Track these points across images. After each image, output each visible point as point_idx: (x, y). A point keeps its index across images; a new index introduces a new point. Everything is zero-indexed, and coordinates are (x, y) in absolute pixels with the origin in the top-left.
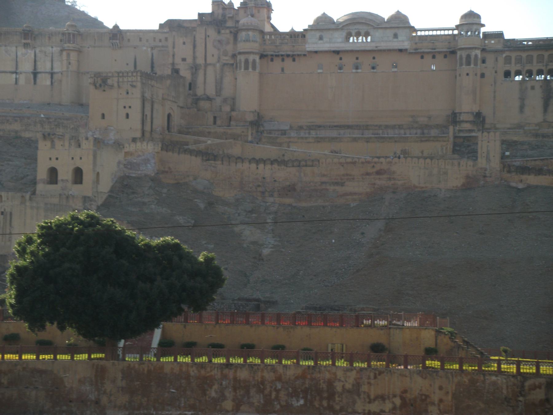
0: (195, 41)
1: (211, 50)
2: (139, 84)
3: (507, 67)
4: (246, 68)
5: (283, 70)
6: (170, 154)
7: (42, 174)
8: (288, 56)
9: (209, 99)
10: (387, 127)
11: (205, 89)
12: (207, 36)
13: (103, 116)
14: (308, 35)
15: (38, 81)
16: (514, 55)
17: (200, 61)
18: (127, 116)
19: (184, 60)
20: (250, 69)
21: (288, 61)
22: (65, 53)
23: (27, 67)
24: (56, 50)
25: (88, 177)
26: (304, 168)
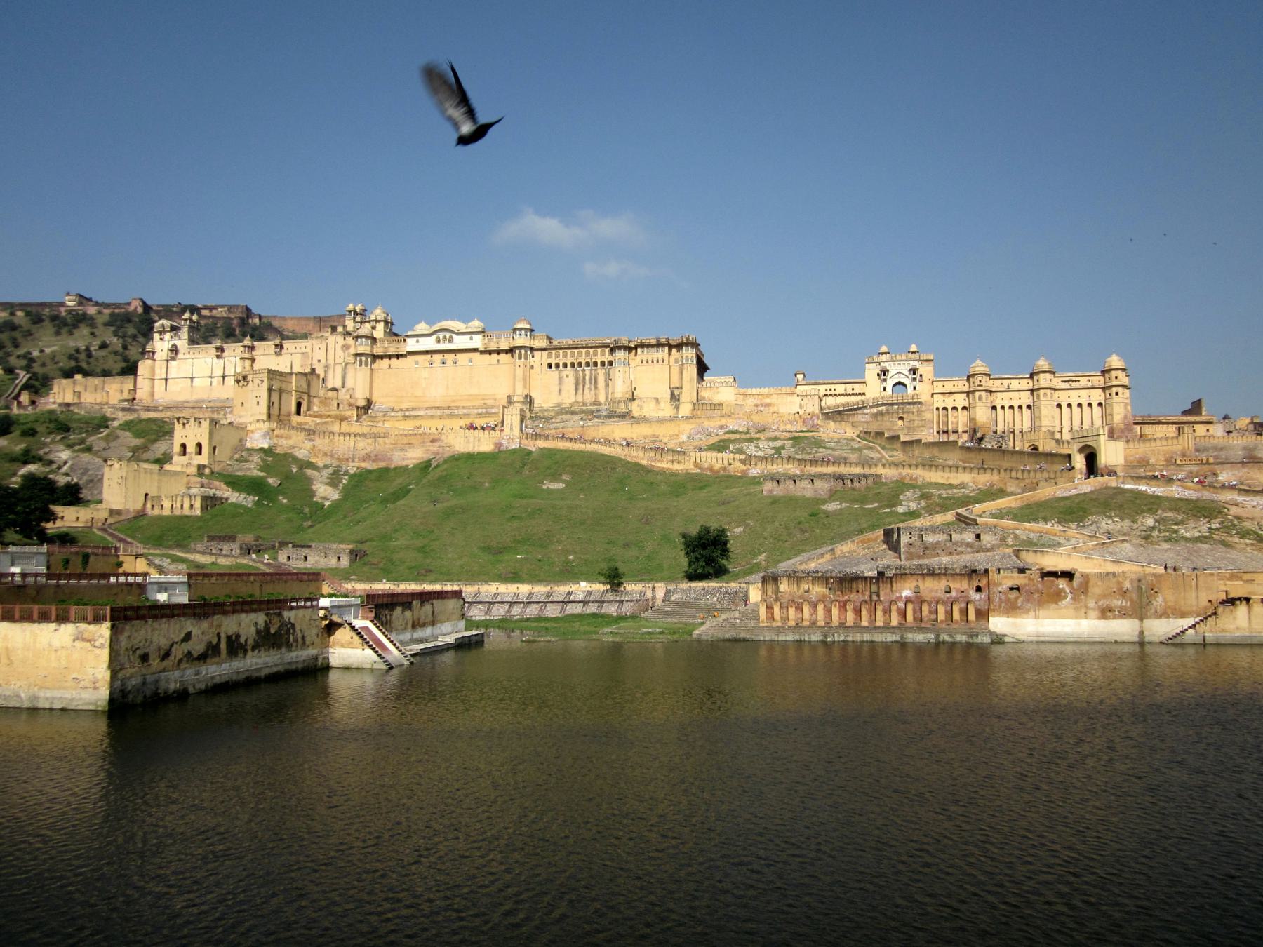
1: (339, 352)
2: (266, 380)
3: (549, 361)
7: (177, 448)
9: (334, 389)
12: (336, 342)
14: (408, 340)
17: (331, 361)
21: (394, 361)
23: (219, 373)
25: (205, 449)
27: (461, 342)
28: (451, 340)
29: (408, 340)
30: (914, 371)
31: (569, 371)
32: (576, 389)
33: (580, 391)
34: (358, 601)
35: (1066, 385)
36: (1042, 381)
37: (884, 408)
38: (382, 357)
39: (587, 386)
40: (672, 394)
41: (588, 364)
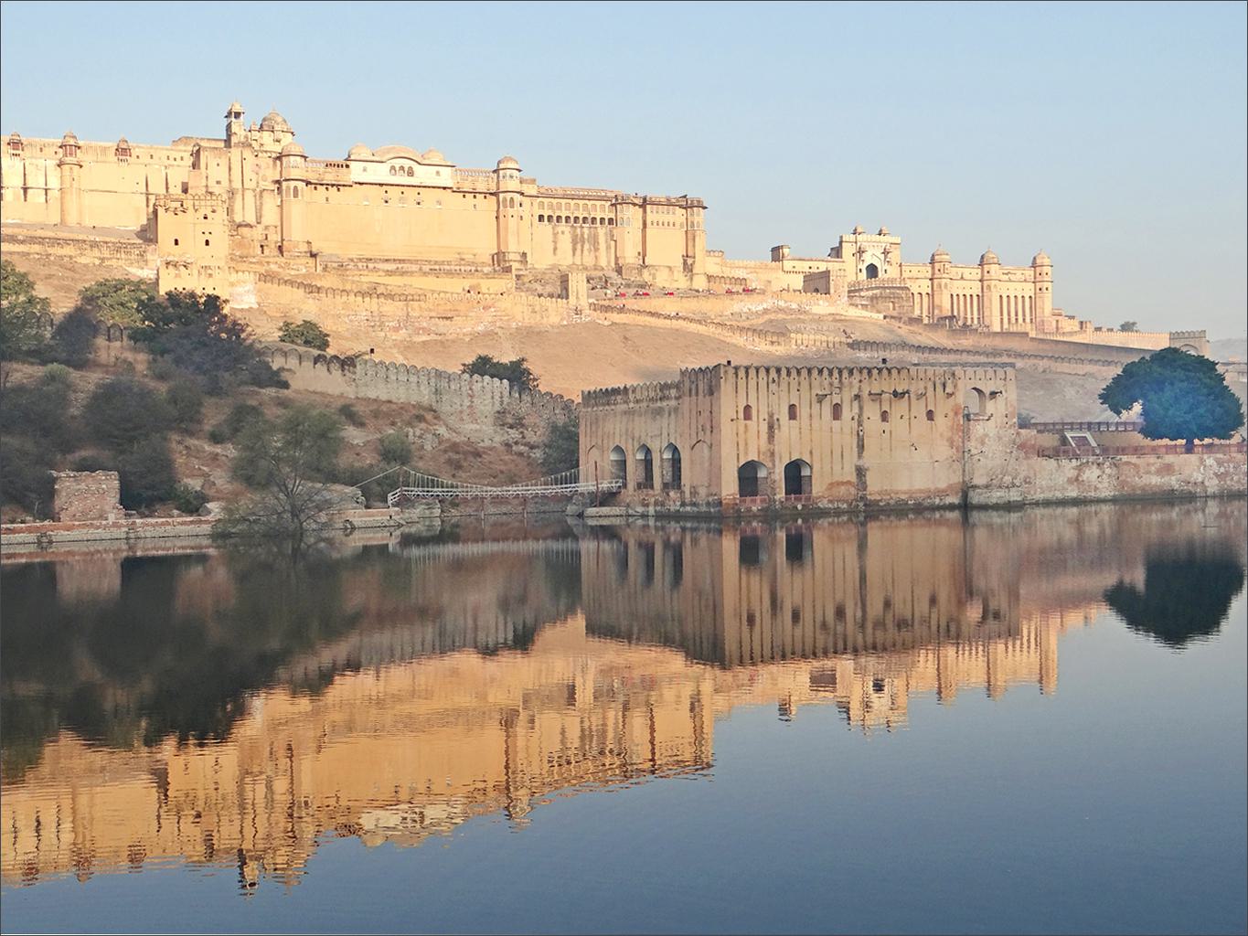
0: (230, 163)
4: (296, 195)
5: (327, 199)
6: (269, 285)
8: (333, 185)
10: (436, 263)
11: (244, 216)
13: (176, 242)
14: (352, 165)
15: (28, 199)
16: (546, 201)
17: (237, 185)
18: (207, 243)
19: (218, 182)
20: (300, 197)
22: (66, 168)
24: (52, 163)
26: (412, 302)
27: (423, 175)
28: (411, 173)
29: (352, 165)
30: (886, 253)
31: (563, 227)
32: (574, 250)
33: (578, 252)
34: (967, 479)
35: (1006, 277)
36: (992, 272)
37: (878, 291)
38: (316, 185)
39: (587, 246)
40: (685, 263)
41: (585, 219)
